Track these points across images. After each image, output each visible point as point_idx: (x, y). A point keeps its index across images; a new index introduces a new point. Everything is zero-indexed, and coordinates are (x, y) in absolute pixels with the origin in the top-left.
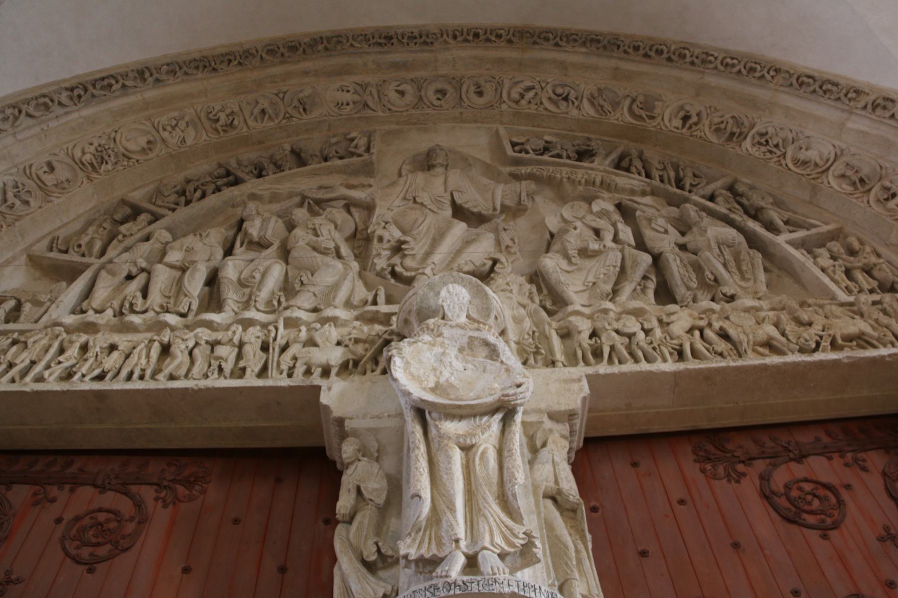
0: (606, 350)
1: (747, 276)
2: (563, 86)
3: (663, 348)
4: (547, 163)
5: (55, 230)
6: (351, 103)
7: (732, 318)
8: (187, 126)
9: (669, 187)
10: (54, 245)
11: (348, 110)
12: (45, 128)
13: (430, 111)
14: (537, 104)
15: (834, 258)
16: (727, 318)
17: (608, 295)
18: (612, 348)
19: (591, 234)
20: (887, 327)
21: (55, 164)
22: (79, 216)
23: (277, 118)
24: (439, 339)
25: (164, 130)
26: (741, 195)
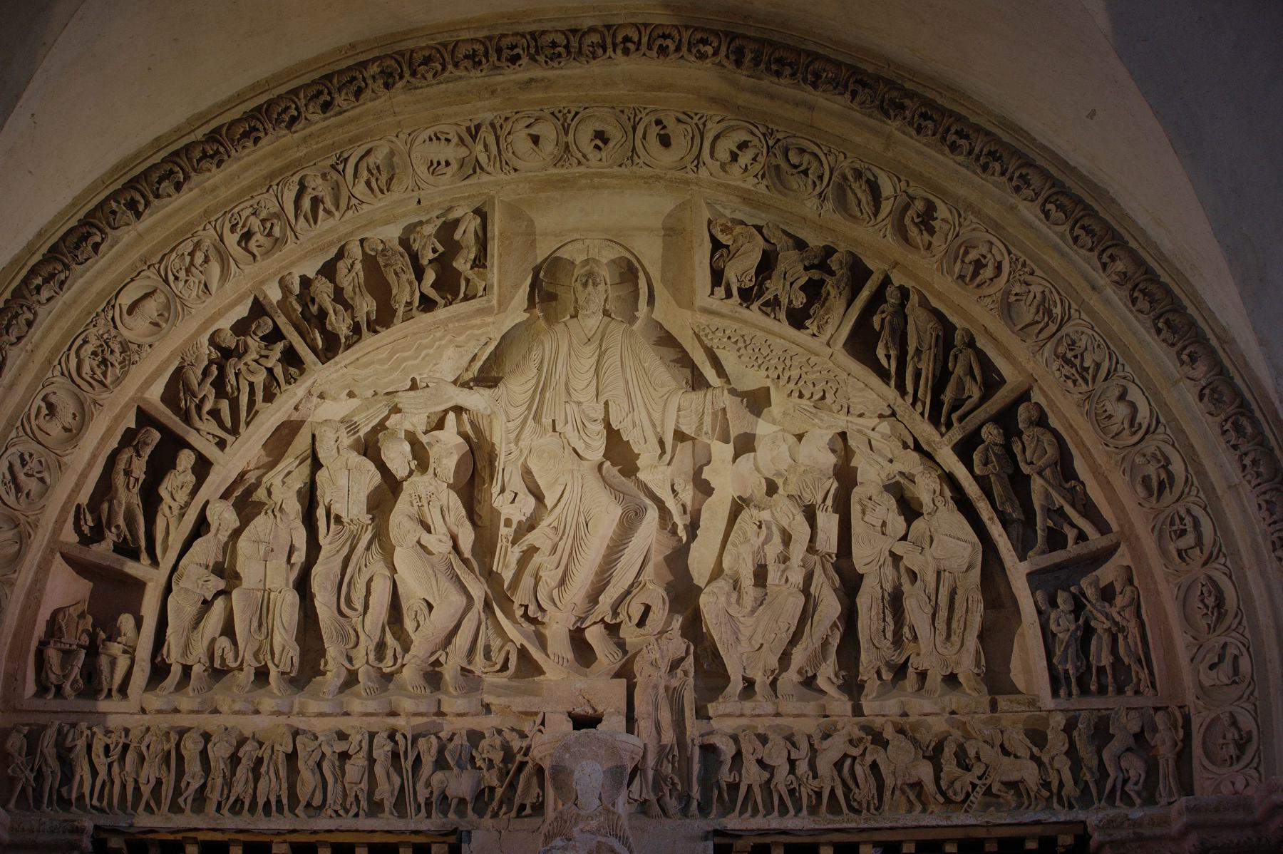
0: (743, 790)
1: (954, 638)
2: (802, 151)
3: (802, 789)
4: (755, 326)
5: (73, 491)
6: (452, 161)
7: (889, 747)
8: (206, 260)
9: (918, 417)
10: (82, 522)
11: (448, 176)
12: (29, 347)
13: (582, 169)
14: (756, 176)
15: (1078, 607)
16: (885, 744)
17: (773, 671)
18: (750, 787)
19: (777, 539)
20: (1058, 771)
21: (53, 399)
22: (94, 457)
23: (337, 208)
24: (571, 843)
25: (176, 278)
26: (1019, 434)
